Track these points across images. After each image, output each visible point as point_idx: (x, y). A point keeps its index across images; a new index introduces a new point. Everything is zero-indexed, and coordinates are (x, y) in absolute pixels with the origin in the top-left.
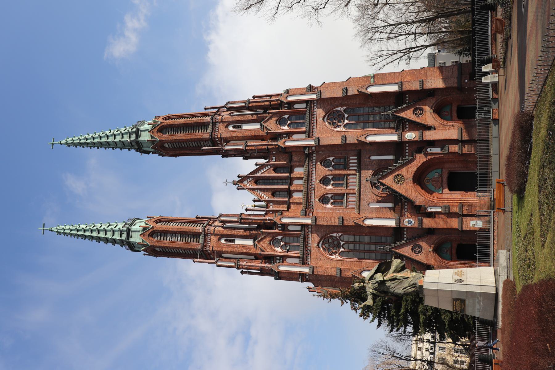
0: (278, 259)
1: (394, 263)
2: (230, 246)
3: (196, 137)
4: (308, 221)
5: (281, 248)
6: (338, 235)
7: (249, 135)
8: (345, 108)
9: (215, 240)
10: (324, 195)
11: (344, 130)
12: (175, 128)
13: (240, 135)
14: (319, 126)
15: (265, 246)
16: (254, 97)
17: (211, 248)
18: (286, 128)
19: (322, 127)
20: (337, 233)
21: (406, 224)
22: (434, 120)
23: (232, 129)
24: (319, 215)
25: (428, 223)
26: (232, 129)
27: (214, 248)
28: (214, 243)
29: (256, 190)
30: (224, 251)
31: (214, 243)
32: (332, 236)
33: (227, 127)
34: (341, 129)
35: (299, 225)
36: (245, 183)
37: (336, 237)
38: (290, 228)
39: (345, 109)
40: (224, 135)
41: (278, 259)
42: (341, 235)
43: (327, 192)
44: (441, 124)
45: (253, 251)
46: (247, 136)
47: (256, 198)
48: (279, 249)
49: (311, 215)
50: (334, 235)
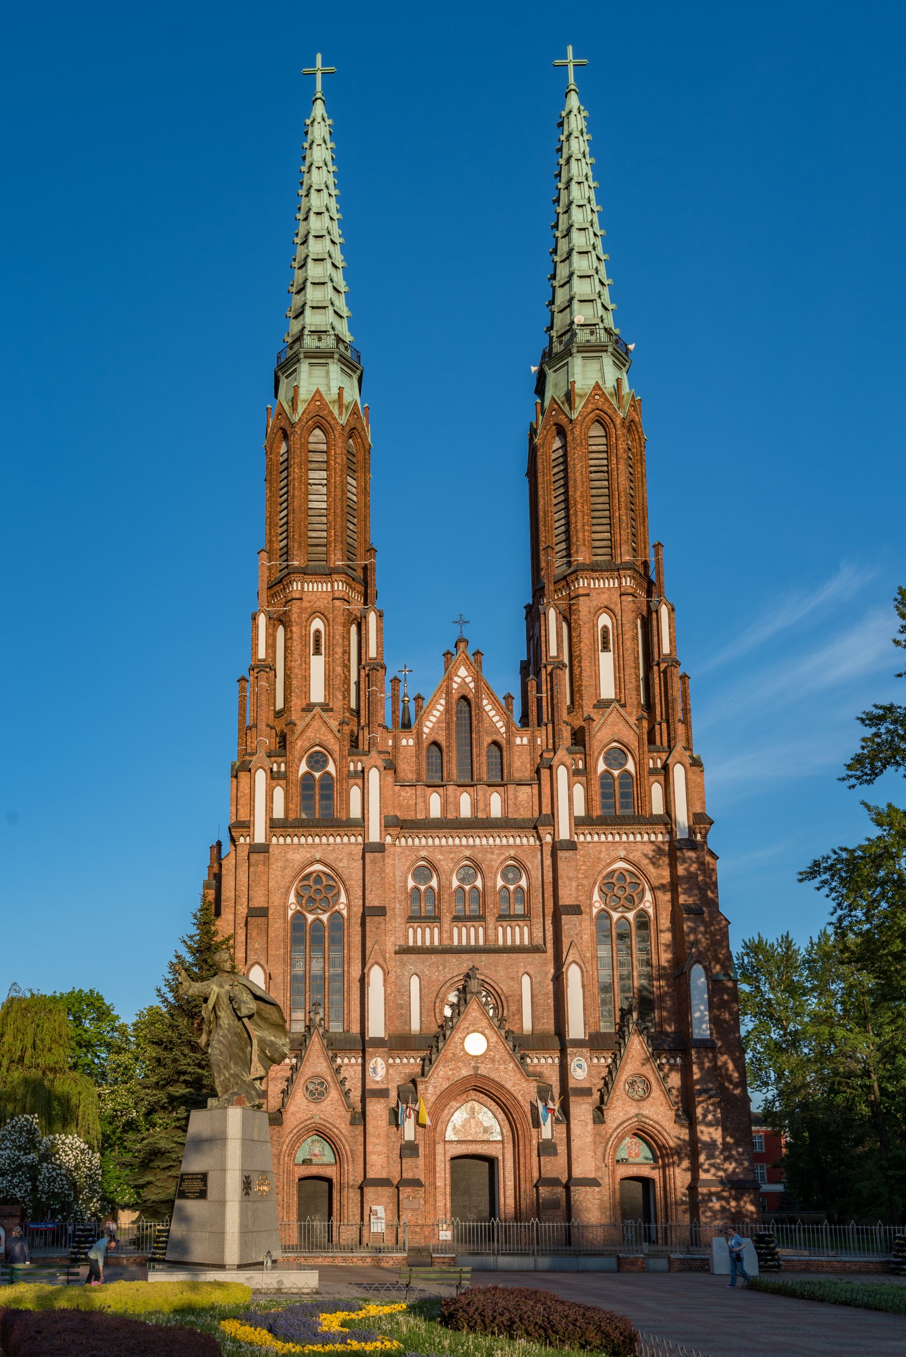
0: (279, 767)
1: (281, 1039)
2: (306, 645)
3: (579, 526)
4: (374, 835)
5: (307, 773)
6: (342, 906)
7: (584, 674)
8: (651, 911)
9: (317, 604)
10: (436, 870)
11: (595, 911)
12: (605, 462)
13: (585, 646)
14: (604, 849)
15: (309, 733)
16: (684, 677)
17: (298, 596)
18: (601, 767)
19: (602, 855)
20: (349, 906)
21: (373, 1061)
22: (618, 1122)
23: (600, 627)
24: (389, 861)
25: (378, 1110)
26: (600, 627)
27: (298, 602)
28: (310, 602)
29: (443, 702)
30: (291, 631)
31: (310, 602)
32: (338, 893)
33: (608, 609)
34: (597, 903)
35: (363, 818)
36: (463, 672)
37: (336, 902)
38: (355, 793)
39: (646, 912)
40: (584, 607)
41: (279, 767)
42: (342, 915)
43: (443, 877)
44: (609, 1140)
45: (297, 703)
46: (580, 667)
47: (425, 704)
48: (303, 768)
49: (389, 839)
50: (343, 898)
